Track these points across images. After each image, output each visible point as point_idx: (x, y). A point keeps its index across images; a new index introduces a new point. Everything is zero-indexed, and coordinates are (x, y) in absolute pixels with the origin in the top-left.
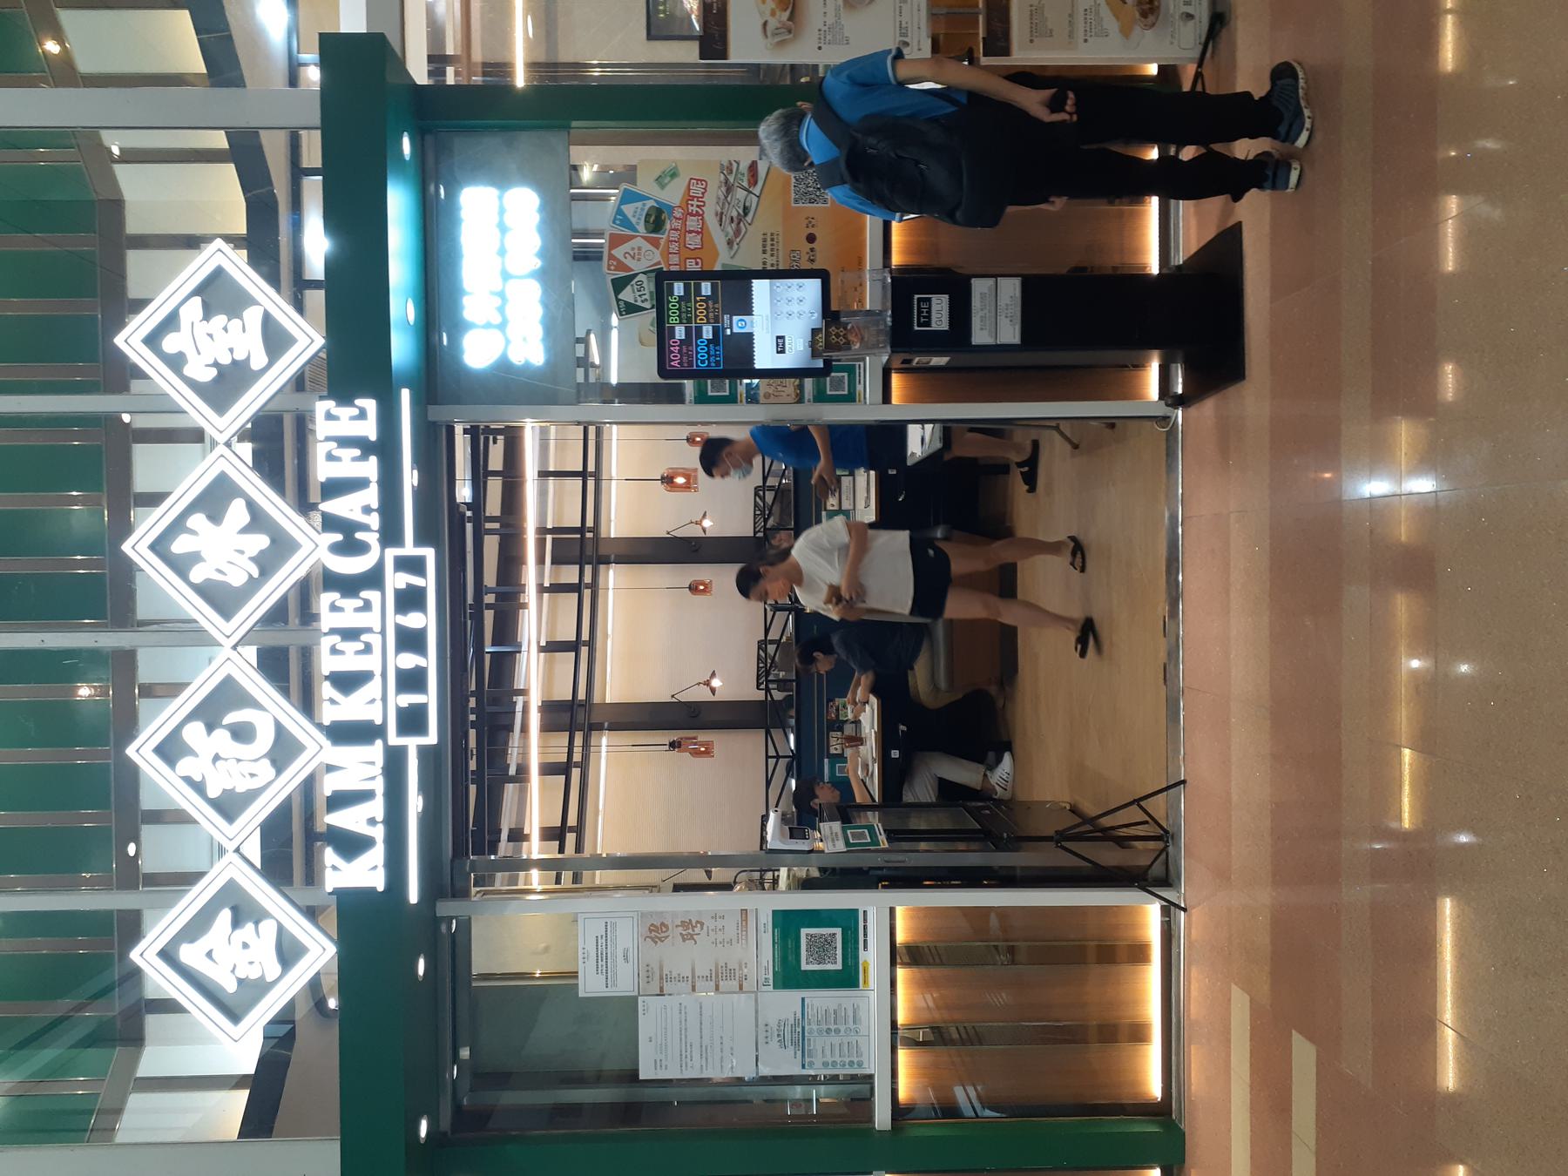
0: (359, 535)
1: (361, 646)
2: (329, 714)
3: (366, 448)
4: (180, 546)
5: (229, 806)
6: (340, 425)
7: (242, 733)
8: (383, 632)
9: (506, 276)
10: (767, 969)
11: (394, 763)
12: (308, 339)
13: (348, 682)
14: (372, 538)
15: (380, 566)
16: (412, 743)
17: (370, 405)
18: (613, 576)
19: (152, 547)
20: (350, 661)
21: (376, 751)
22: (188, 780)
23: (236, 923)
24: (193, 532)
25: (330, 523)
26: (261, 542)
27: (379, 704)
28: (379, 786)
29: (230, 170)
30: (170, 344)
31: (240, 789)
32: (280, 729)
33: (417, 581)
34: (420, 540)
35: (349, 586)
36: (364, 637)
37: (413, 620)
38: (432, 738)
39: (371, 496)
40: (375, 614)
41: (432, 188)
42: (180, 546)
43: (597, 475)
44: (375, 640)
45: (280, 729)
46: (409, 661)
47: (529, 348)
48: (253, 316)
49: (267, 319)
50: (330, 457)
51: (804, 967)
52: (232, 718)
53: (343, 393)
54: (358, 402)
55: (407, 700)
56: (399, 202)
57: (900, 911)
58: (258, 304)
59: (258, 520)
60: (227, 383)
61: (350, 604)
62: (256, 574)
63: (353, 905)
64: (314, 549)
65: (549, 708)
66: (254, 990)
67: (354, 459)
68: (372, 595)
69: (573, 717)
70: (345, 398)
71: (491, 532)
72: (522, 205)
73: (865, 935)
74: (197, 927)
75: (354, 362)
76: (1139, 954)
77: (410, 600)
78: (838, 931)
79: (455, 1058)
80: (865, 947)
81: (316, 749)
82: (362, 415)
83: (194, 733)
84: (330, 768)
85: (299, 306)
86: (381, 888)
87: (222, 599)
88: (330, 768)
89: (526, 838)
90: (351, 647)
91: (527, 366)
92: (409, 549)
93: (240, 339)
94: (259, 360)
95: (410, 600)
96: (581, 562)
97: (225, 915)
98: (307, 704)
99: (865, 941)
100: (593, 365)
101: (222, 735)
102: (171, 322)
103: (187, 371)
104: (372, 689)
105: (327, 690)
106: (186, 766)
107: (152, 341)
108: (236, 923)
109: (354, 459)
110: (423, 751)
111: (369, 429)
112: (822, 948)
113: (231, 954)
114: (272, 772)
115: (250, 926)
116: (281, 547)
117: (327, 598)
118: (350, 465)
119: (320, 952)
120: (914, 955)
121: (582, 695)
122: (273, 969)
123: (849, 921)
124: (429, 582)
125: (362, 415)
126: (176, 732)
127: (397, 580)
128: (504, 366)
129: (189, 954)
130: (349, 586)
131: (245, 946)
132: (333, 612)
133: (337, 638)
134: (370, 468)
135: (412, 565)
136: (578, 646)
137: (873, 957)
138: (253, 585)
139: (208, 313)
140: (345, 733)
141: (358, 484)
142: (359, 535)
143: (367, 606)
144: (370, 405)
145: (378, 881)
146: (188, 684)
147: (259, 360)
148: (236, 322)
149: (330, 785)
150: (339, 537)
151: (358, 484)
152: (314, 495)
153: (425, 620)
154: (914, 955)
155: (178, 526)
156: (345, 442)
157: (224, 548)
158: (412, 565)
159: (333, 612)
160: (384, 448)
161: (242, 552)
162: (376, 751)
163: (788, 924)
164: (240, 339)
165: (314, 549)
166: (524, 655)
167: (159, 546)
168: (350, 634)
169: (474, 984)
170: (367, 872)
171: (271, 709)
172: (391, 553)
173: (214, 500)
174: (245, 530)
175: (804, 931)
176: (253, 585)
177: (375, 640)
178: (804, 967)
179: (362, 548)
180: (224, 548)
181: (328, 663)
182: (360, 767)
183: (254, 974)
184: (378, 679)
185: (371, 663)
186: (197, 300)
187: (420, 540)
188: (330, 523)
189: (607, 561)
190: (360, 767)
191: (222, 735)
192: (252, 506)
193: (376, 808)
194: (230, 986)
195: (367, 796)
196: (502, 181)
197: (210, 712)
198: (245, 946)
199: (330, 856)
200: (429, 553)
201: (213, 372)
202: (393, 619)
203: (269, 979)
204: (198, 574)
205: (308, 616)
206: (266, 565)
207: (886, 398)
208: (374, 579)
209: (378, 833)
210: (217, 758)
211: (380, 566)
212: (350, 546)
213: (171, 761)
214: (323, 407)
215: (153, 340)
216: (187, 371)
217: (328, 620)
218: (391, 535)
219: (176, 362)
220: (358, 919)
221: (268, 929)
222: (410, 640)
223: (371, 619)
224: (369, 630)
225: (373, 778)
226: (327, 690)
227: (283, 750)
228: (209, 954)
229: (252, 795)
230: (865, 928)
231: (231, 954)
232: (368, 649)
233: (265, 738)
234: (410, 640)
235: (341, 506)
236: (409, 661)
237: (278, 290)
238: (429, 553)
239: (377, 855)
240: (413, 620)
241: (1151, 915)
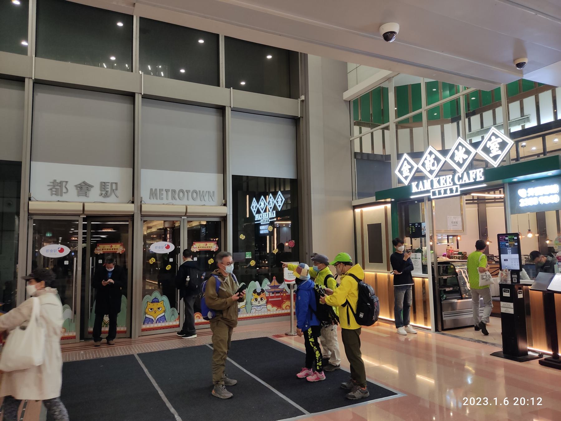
3: (475, 179)
4: (460, 147)
5: (423, 165)
6: (478, 174)
11: (428, 191)
12: (495, 164)
13: (439, 182)
14: (461, 183)
16: (431, 194)
17: (483, 179)
20: (442, 181)
25: (463, 174)
26: (461, 162)
28: (425, 189)
30: (493, 138)
32: (434, 171)
33: (454, 191)
35: (453, 180)
37: (448, 192)
38: (432, 197)
39: (467, 181)
40: (449, 185)
42: (460, 147)
45: (434, 171)
46: (442, 192)
47: (523, 203)
48: (499, 152)
49: (500, 155)
52: (435, 162)
53: (485, 174)
54: (483, 177)
59: (464, 161)
60: (487, 150)
61: (450, 180)
63: (409, 187)
64: (460, 171)
74: (409, 163)
76: (426, 324)
77: (451, 191)
82: (481, 178)
87: (452, 157)
91: (520, 203)
92: (459, 189)
93: (495, 151)
94: (491, 155)
101: (432, 161)
102: (497, 137)
110: (430, 196)
111: (478, 179)
118: (472, 176)
125: (481, 178)
127: (454, 188)
128: (520, 198)
130: (453, 180)
132: (449, 177)
134: (472, 180)
135: (457, 191)
138: (454, 161)
139: (499, 143)
140: (432, 182)
141: (469, 179)
146: (450, 150)
147: (491, 155)
148: (498, 149)
151: (469, 180)
153: (449, 194)
154: (424, 283)
156: (476, 175)
158: (457, 191)
160: (476, 183)
164: (495, 151)
170: (414, 189)
171: (437, 169)
172: (458, 186)
177: (445, 185)
179: (459, 181)
181: (441, 178)
182: (427, 186)
186: (501, 141)
187: (461, 191)
188: (463, 174)
192: (467, 159)
193: (423, 190)
199: (416, 183)
202: (448, 188)
204: (456, 151)
208: (454, 184)
209: (419, 190)
212: (459, 179)
214: (482, 170)
218: (462, 186)
219: (490, 139)
226: (438, 178)
227: (431, 172)
229: (425, 168)
233: (433, 168)
236: (442, 192)
238: (459, 193)
240: (448, 192)
241: (429, 327)
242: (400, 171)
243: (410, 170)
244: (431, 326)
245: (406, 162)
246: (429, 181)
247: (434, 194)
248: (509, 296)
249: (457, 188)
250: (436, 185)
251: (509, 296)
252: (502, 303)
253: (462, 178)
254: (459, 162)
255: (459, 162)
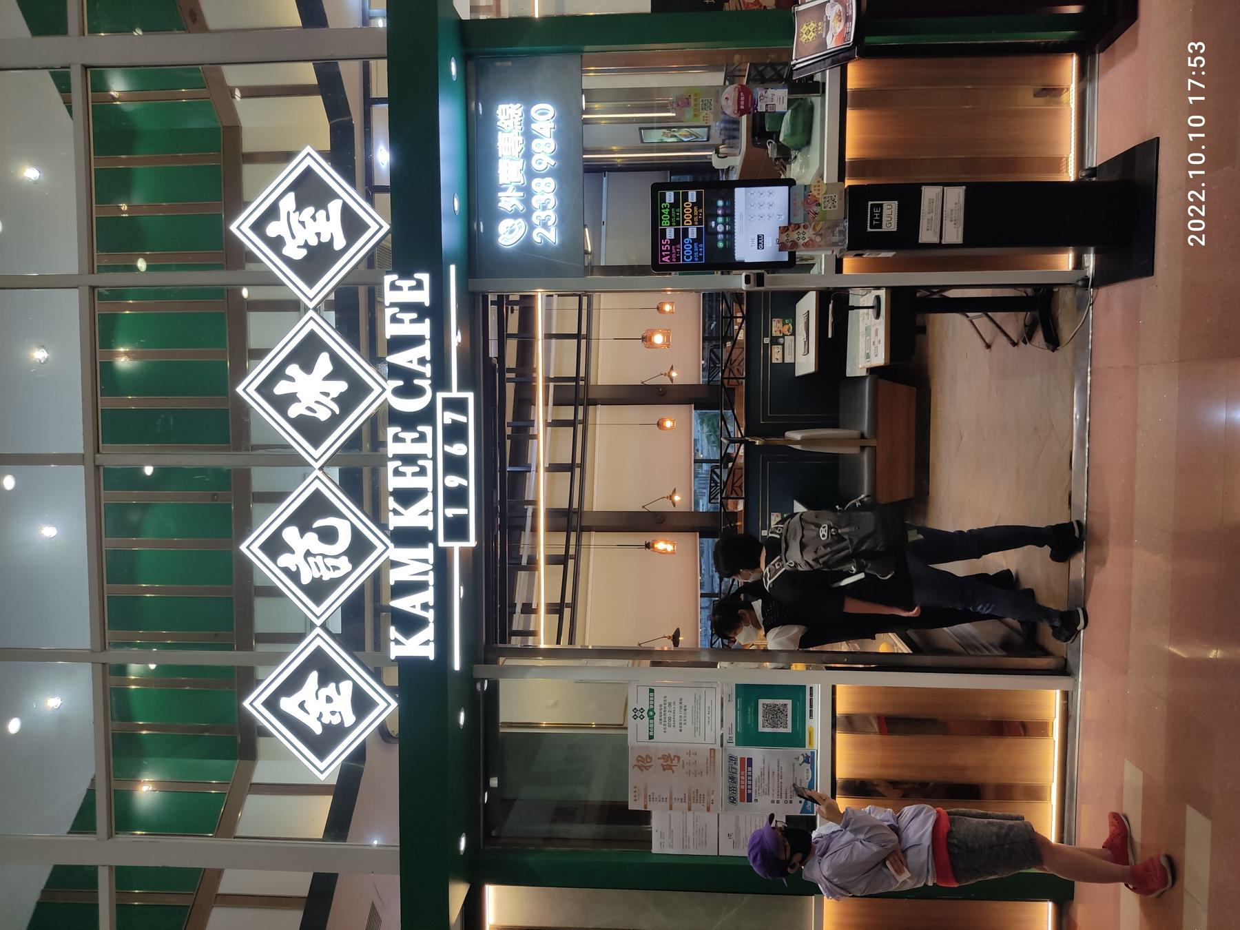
0: (417, 382)
1: (417, 469)
2: (394, 522)
3: (421, 312)
4: (281, 388)
5: (318, 590)
6: (403, 291)
7: (328, 536)
8: (434, 459)
9: (530, 174)
10: (730, 730)
11: (442, 560)
12: (378, 225)
13: (408, 497)
14: (426, 384)
15: (432, 406)
16: (456, 546)
17: (425, 277)
18: (602, 416)
19: (258, 390)
21: (428, 552)
22: (286, 571)
23: (323, 682)
24: (291, 379)
26: (341, 386)
27: (431, 514)
28: (430, 578)
29: (317, 102)
30: (273, 230)
31: (325, 578)
32: (355, 530)
33: (461, 418)
34: (461, 387)
35: (408, 421)
36: (420, 462)
37: (458, 449)
39: (425, 350)
41: (473, 105)
42: (281, 388)
43: (588, 337)
44: (428, 464)
45: (355, 532)
46: (454, 481)
47: (549, 235)
48: (335, 207)
49: (346, 209)
50: (394, 319)
51: (761, 729)
52: (318, 524)
55: (451, 512)
56: (449, 116)
57: (839, 688)
58: (338, 197)
60: (317, 260)
62: (337, 411)
64: (382, 392)
65: (552, 513)
66: (334, 734)
67: (412, 321)
68: (427, 429)
69: (569, 520)
70: (406, 274)
71: (510, 380)
72: (545, 116)
73: (811, 706)
74: (293, 684)
75: (413, 245)
77: (455, 433)
78: (789, 702)
79: (487, 787)
80: (811, 715)
81: (384, 550)
83: (291, 534)
84: (395, 564)
85: (369, 199)
86: (432, 658)
87: (313, 430)
88: (395, 564)
89: (535, 611)
90: (409, 470)
92: (455, 393)
93: (325, 226)
94: (339, 243)
95: (455, 433)
96: (576, 403)
97: (314, 677)
98: (377, 515)
99: (811, 711)
100: (586, 252)
101: (312, 537)
102: (272, 213)
103: (286, 251)
104: (426, 503)
105: (392, 503)
106: (285, 560)
107: (259, 227)
108: (323, 682)
109: (412, 321)
111: (424, 297)
112: (775, 714)
113: (318, 705)
114: (349, 567)
115: (332, 685)
116: (358, 390)
117: (392, 431)
119: (386, 706)
120: (851, 723)
121: (575, 505)
122: (349, 719)
123: (797, 693)
124: (470, 419)
125: (419, 286)
126: (278, 534)
127: (446, 418)
128: (527, 245)
129: (288, 704)
130: (408, 421)
131: (329, 700)
133: (399, 463)
134: (424, 329)
135: (457, 406)
136: (572, 468)
137: (817, 725)
138: (335, 421)
139: (300, 207)
140: (408, 537)
141: (416, 341)
142: (417, 382)
143: (422, 438)
144: (425, 277)
145: (430, 652)
147: (339, 243)
148: (322, 213)
149: (395, 576)
150: (401, 383)
151: (416, 341)
152: (382, 349)
153: (465, 449)
154: (851, 723)
155: (278, 374)
156: (405, 307)
157: (313, 390)
158: (457, 406)
159: (399, 442)
160: (435, 312)
161: (327, 394)
162: (428, 552)
163: (748, 695)
164: (325, 226)
165: (382, 392)
166: (533, 473)
167: (265, 389)
168: (409, 460)
169: (502, 730)
170: (420, 646)
171: (348, 520)
172: (440, 396)
173: (306, 353)
174: (329, 377)
175: (761, 702)
176: (335, 421)
177: (428, 464)
178: (761, 729)
179: (419, 392)
180: (313, 390)
182: (414, 563)
183: (336, 720)
184: (430, 495)
185: (425, 482)
186: (291, 196)
187: (461, 387)
188: (395, 372)
189: (594, 403)
190: (414, 563)
191: (312, 537)
192: (335, 358)
193: (428, 596)
194: (318, 730)
195: (421, 586)
196: (528, 99)
197: (303, 519)
198: (329, 700)
199: (393, 633)
200: (470, 396)
201: (304, 252)
203: (347, 725)
204: (294, 411)
205: (378, 444)
206: (347, 402)
207: (839, 269)
208: (427, 415)
209: (430, 615)
210: (308, 554)
211: (432, 406)
213: (273, 557)
215: (259, 227)
216: (286, 251)
217: (393, 449)
218: (440, 382)
219: (276, 244)
220: (415, 681)
221: (346, 687)
222: (455, 465)
223: (425, 448)
224: (424, 457)
225: (426, 573)
227: (359, 549)
228: (302, 705)
229: (335, 583)
230: (811, 700)
231: (318, 705)
232: (423, 472)
233: (345, 540)
234: (455, 465)
235: (401, 359)
236: (454, 481)
237: (353, 184)
238: (470, 396)
239: (429, 633)
240: (458, 449)
242: (321, 743)
243: (330, 674)
244: (1049, 701)
245: (288, 704)
246: (397, 554)
247: (456, 528)
248: (895, 204)
249: (450, 405)
250: (412, 517)
251: (895, 204)
252: (927, 235)
253: (406, 375)
254: (339, 400)
255: (339, 400)
